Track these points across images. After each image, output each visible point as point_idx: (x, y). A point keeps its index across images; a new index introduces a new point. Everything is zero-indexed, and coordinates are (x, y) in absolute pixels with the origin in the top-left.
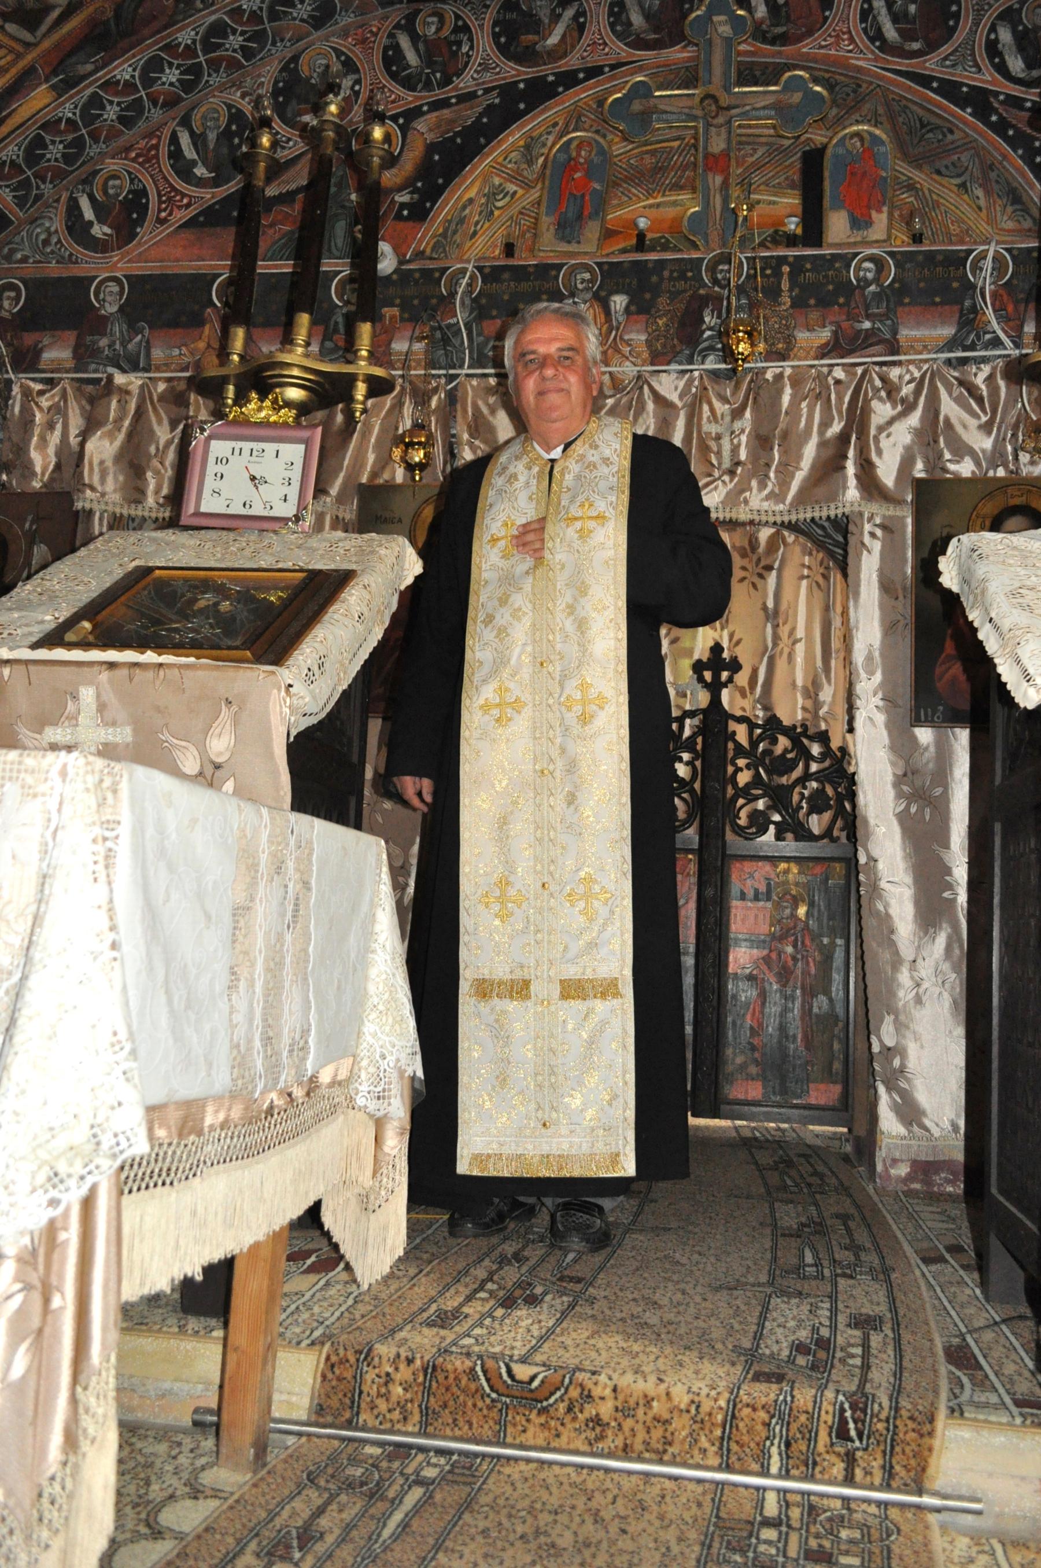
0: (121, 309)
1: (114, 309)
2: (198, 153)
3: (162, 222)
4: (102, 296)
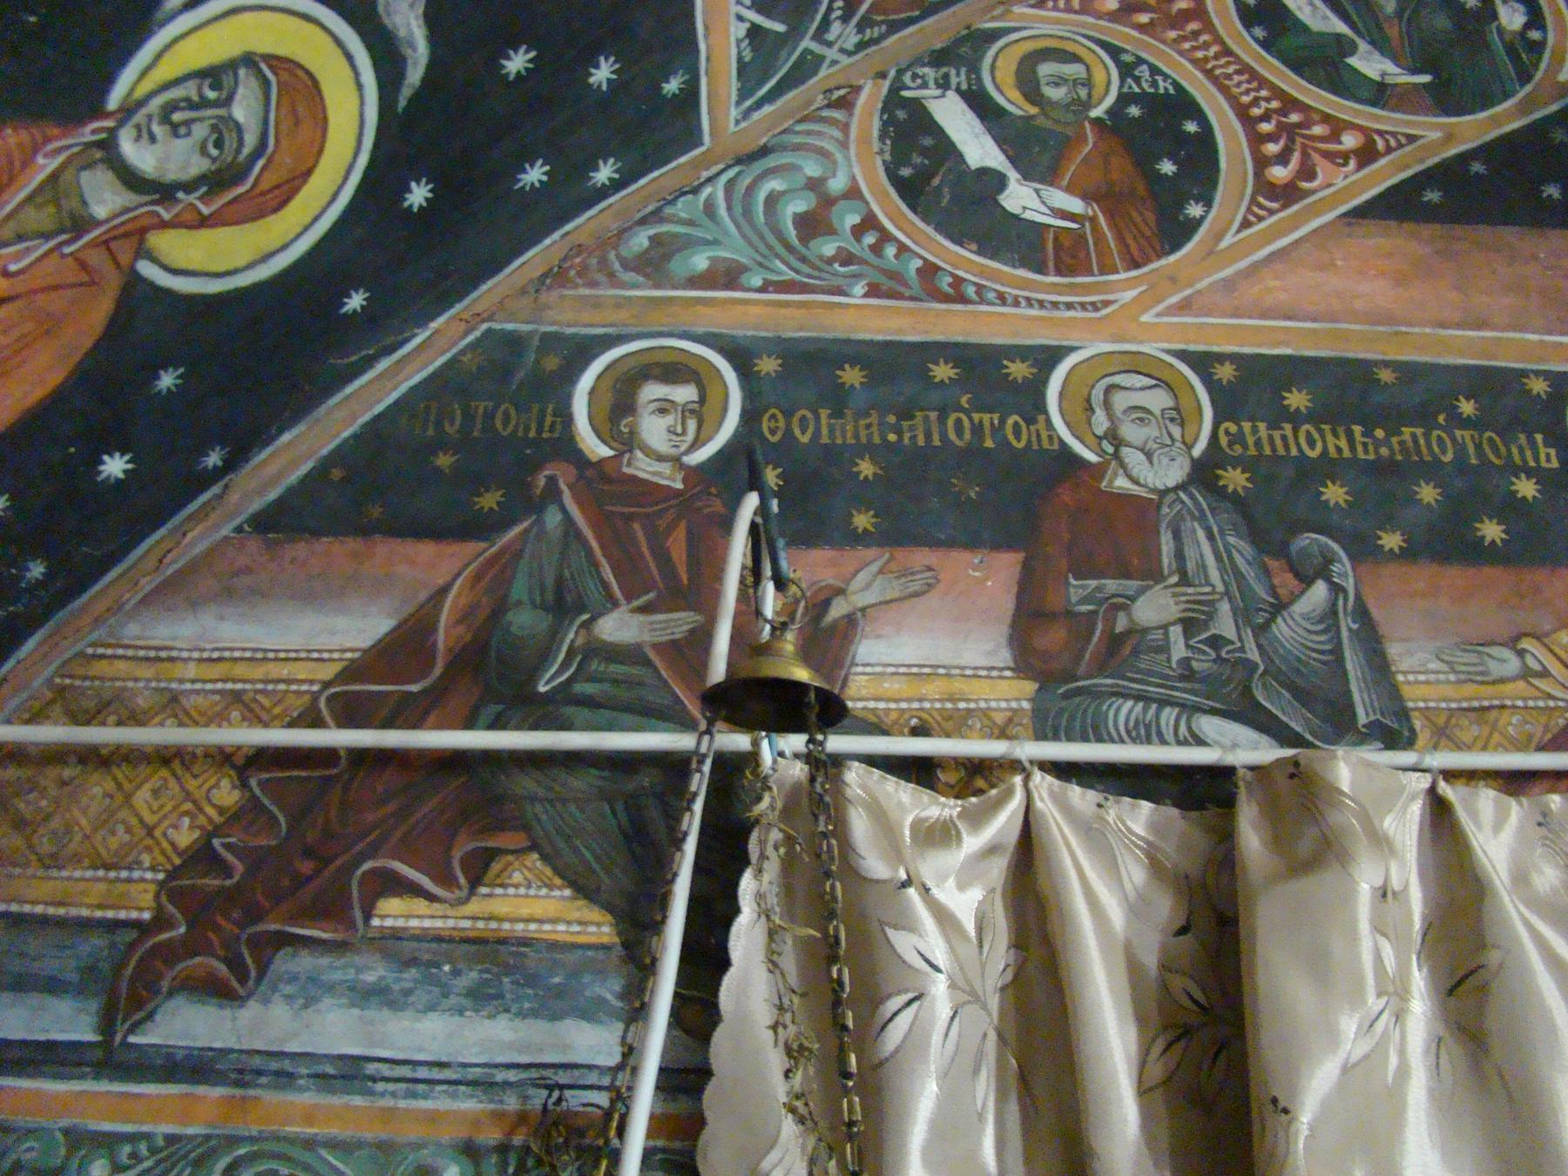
0: (1204, 474)
1: (1171, 473)
2: (1345, 17)
3: (1287, 194)
4: (1101, 422)
